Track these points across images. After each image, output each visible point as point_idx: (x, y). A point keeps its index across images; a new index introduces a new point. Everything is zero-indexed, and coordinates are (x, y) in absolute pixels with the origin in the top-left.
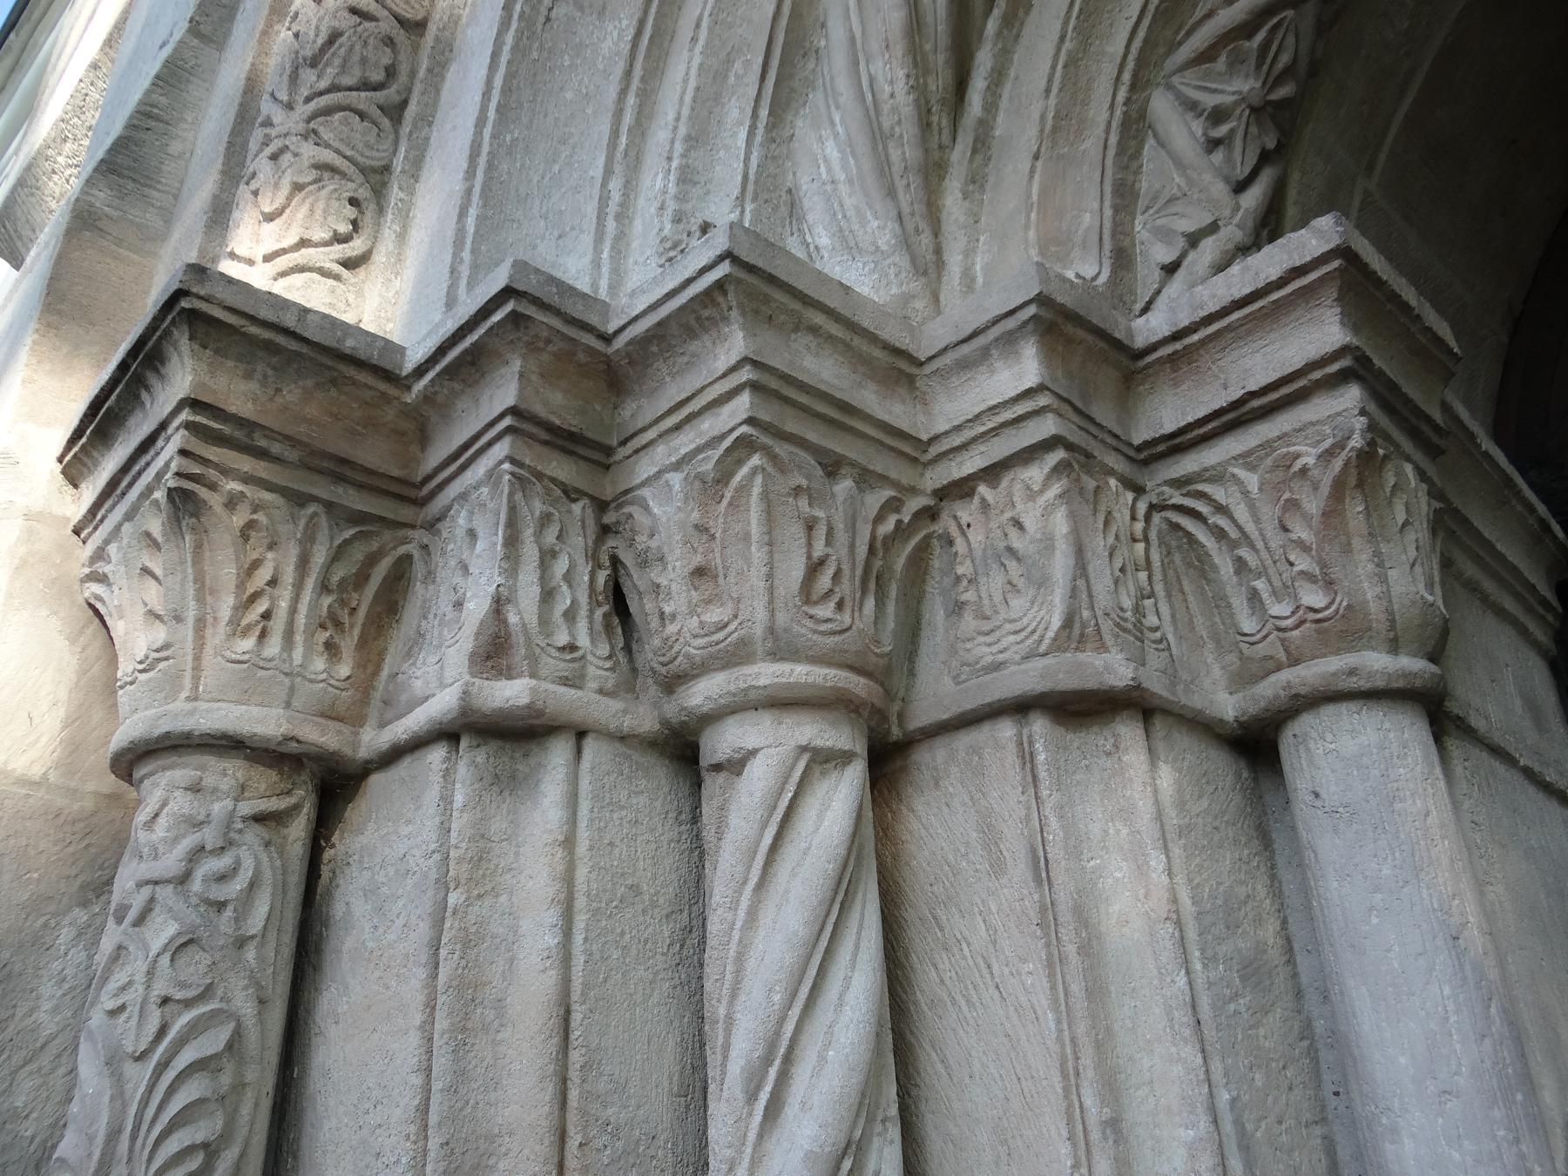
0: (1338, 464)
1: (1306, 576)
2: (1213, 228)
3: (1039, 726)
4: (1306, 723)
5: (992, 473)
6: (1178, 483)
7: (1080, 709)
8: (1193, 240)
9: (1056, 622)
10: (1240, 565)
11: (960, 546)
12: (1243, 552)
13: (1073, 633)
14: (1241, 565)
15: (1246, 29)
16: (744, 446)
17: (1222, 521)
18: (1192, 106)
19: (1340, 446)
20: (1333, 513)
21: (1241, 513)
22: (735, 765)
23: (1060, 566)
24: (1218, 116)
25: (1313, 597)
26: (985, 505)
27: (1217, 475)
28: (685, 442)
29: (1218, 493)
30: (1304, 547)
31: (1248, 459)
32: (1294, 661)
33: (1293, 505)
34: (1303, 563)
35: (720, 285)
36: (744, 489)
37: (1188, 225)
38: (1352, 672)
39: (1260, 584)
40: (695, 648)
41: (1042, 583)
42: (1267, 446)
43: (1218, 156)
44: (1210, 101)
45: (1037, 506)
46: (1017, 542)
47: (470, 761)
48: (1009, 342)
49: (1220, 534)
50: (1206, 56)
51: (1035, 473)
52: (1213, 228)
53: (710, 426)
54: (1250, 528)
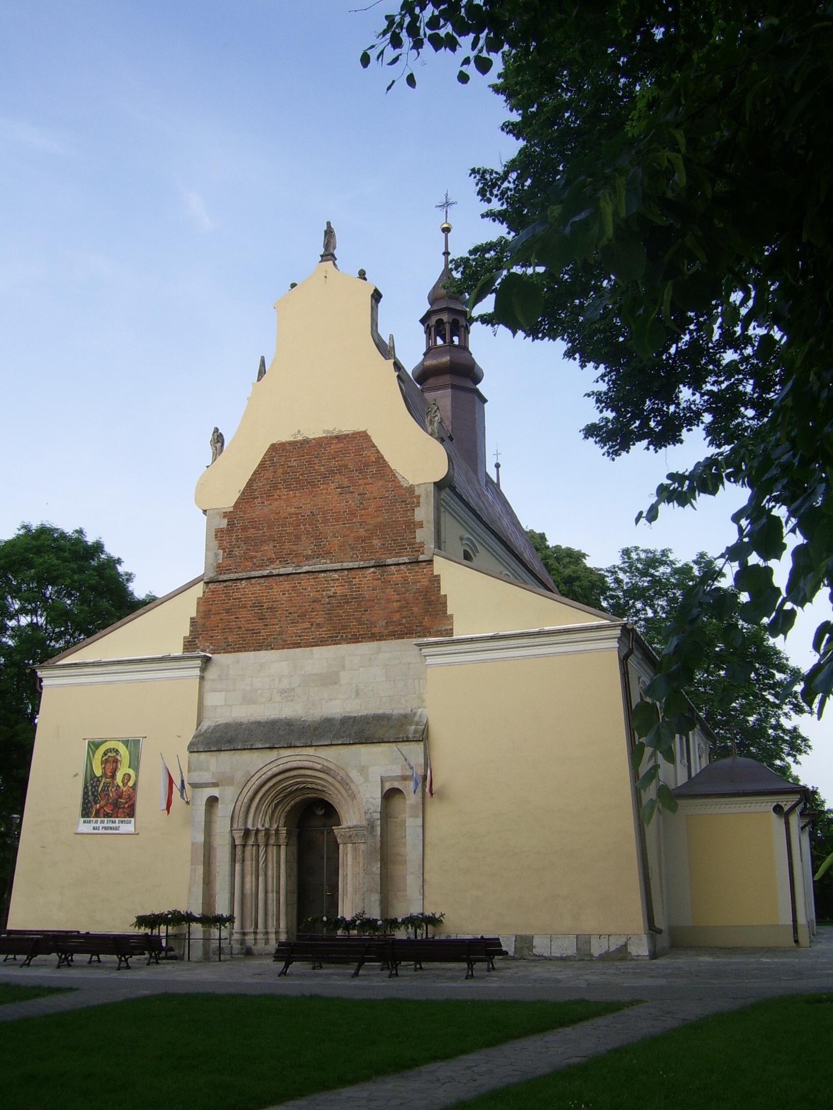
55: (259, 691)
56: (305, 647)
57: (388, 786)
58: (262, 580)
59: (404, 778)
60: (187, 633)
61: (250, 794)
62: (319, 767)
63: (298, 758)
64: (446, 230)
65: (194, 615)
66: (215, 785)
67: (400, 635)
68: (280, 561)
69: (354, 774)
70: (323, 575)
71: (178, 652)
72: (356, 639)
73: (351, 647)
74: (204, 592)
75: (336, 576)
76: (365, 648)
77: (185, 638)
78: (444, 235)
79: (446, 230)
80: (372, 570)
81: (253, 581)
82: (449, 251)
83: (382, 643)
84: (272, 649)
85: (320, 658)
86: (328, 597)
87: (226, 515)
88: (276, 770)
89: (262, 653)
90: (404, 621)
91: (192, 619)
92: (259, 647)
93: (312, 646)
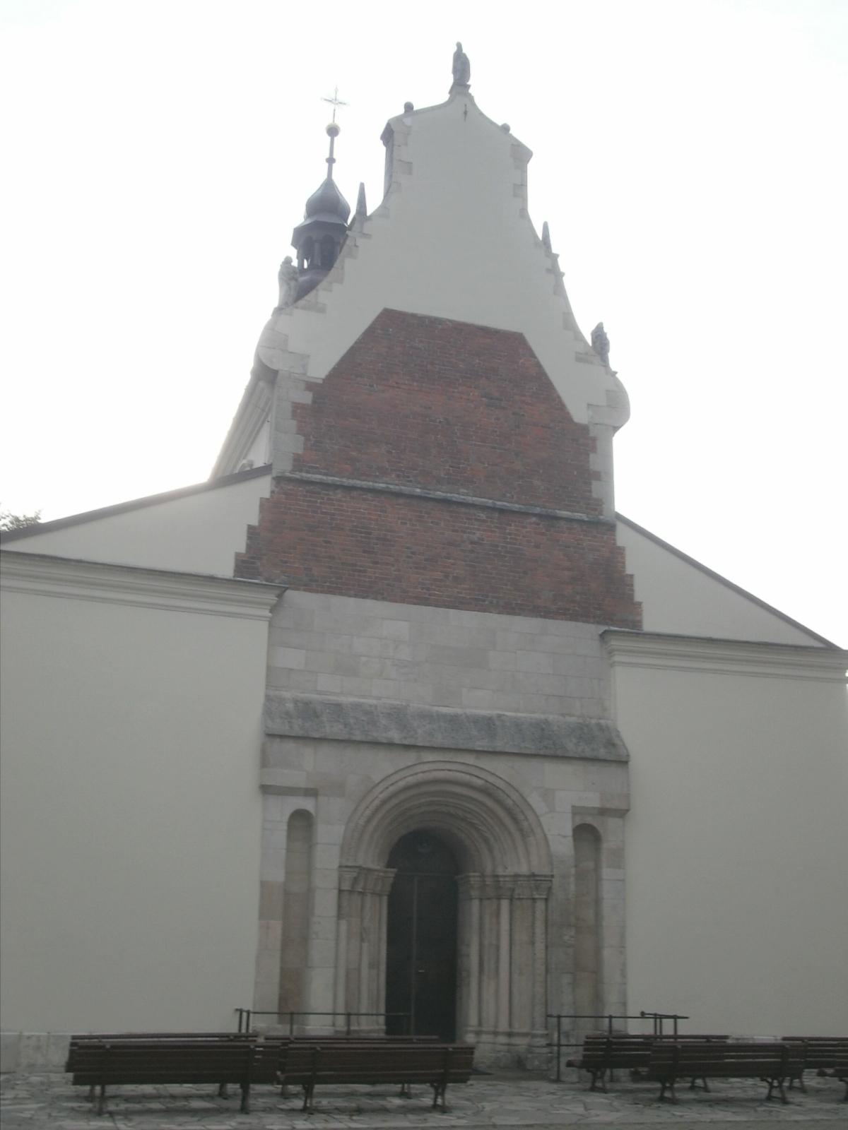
55: (364, 659)
56: (436, 606)
57: (578, 821)
58: (369, 496)
59: (603, 812)
60: (242, 548)
62: (479, 782)
63: (448, 766)
64: (333, 131)
65: (255, 521)
66: (311, 793)
67: (574, 617)
68: (398, 476)
69: (535, 800)
70: (463, 510)
71: (226, 569)
72: (510, 609)
73: (505, 619)
74: (273, 492)
75: (483, 516)
76: (524, 624)
77: (237, 555)
78: (329, 138)
79: (333, 131)
80: (534, 519)
81: (355, 493)
82: (335, 157)
83: (549, 622)
84: (384, 599)
85: (460, 626)
86: (472, 543)
87: (310, 386)
88: (411, 780)
89: (369, 603)
90: (578, 597)
91: (250, 528)
92: (366, 591)
93: (448, 607)
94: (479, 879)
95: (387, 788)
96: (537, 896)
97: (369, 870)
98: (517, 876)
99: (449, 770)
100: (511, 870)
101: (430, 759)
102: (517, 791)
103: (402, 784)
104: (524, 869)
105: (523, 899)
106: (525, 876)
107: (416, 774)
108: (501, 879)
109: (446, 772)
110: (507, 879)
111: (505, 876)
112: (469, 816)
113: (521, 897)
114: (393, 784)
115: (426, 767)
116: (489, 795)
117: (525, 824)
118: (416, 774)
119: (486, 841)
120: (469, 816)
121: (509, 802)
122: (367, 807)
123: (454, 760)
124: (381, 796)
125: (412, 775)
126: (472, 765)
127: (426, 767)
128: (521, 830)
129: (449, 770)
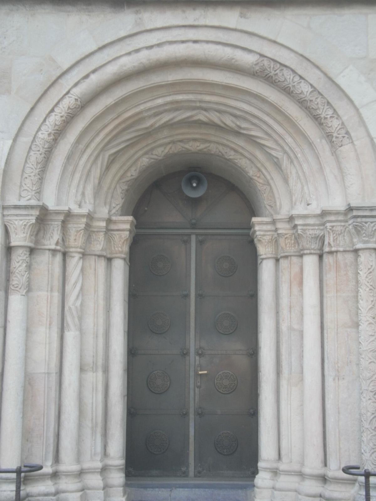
0: (125, 238)
1: (120, 247)
2: (119, 204)
3: (97, 257)
4: (116, 259)
5: (97, 232)
6: (111, 234)
7: (99, 256)
8: (117, 205)
9: (101, 248)
10: (114, 244)
11: (92, 237)
12: (115, 242)
13: (102, 250)
14: (114, 244)
15: (128, 181)
16: (83, 229)
17: (114, 239)
18: (120, 187)
19: (126, 237)
20: (123, 243)
21: (116, 239)
22: (73, 257)
23: (102, 243)
24: (123, 190)
25: (120, 249)
26: (96, 234)
27: (115, 235)
28: (75, 226)
29: (114, 236)
30: (120, 244)
31: (118, 234)
32: (116, 253)
33: (121, 240)
34: (120, 246)
35: (86, 215)
36: (81, 233)
37: (117, 203)
38: (121, 256)
39: (115, 246)
40: (73, 246)
41: (100, 244)
42: (120, 234)
43: (121, 194)
44: (123, 188)
45: (101, 237)
46: (99, 239)
47: (50, 252)
48: (103, 220)
49: (113, 240)
50: (123, 182)
51: (102, 233)
52: (119, 204)
53: (79, 225)
54: (116, 241)
61: (55, 119)
62: (248, 59)
63: (192, 34)
88: (128, 63)
94: (269, 227)
95: (87, 76)
96: (359, 246)
97: (68, 215)
98: (324, 214)
99: (195, 42)
100: (315, 208)
101: (159, 24)
102: (318, 67)
103: (111, 71)
104: (338, 203)
105: (337, 252)
106: (337, 213)
107: (137, 51)
108: (298, 222)
109: (190, 44)
110: (311, 221)
111: (305, 217)
112: (244, 125)
113: (333, 249)
114: (94, 71)
115: (153, 38)
116: (269, 79)
117: (335, 123)
118: (137, 51)
119: (277, 165)
120: (244, 125)
121: (305, 88)
122: (52, 111)
123: (202, 22)
124: (77, 91)
125: (129, 54)
126: (235, 30)
127: (153, 38)
128: (329, 137)
129: (195, 42)
